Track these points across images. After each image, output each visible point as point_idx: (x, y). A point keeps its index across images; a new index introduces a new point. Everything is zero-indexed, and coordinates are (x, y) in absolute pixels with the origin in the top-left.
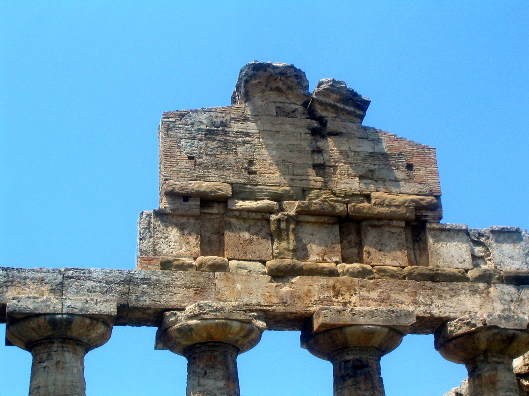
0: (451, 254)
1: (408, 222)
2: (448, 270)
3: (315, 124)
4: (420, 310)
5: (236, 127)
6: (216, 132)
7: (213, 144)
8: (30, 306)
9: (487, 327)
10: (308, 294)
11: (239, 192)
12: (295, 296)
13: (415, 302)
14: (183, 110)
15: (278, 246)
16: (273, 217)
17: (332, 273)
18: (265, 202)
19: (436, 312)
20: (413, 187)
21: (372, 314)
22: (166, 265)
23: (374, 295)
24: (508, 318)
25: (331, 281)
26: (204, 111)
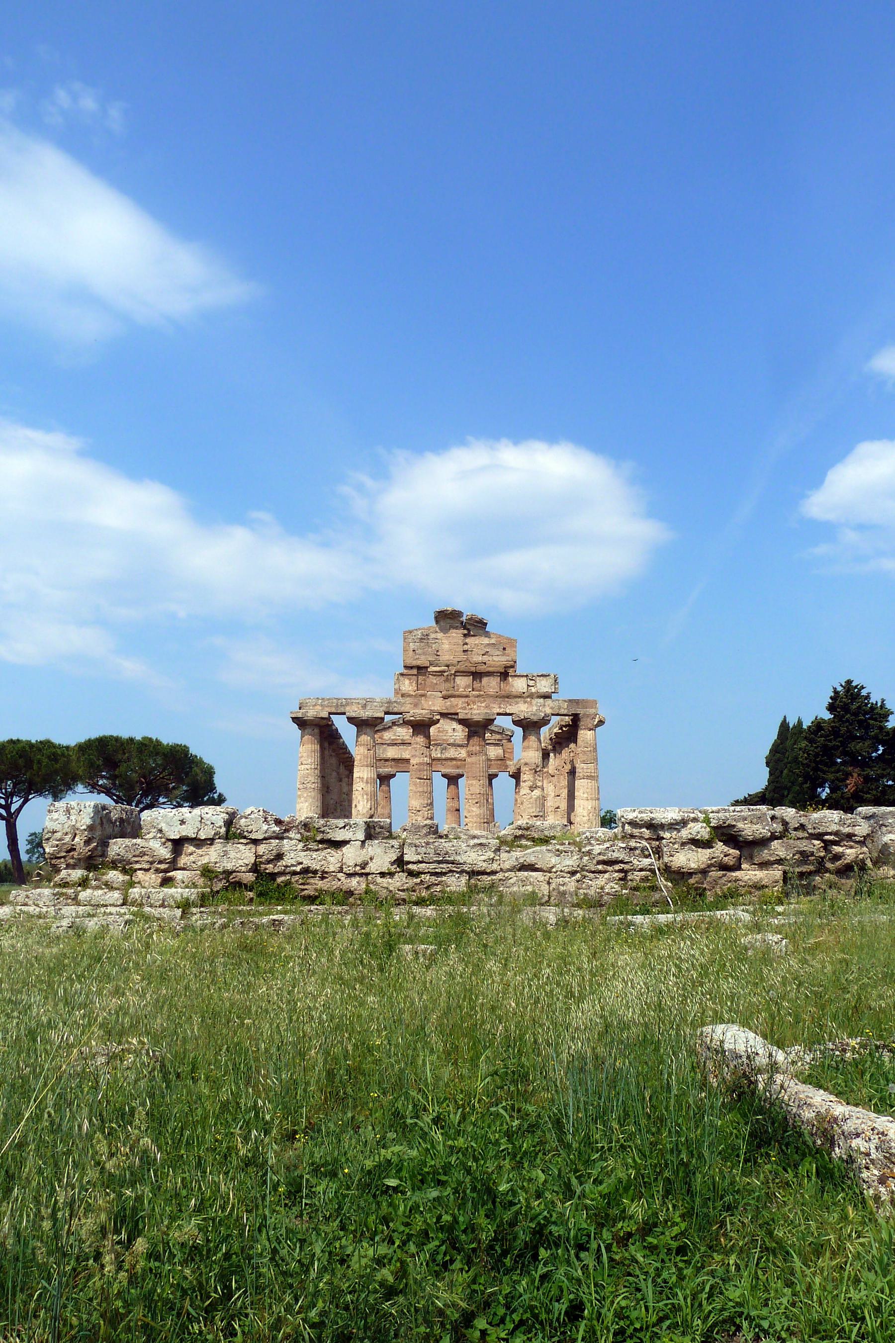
0: (519, 685)
1: (501, 673)
2: (514, 693)
3: (466, 632)
4: (501, 711)
5: (432, 636)
6: (424, 638)
7: (422, 644)
8: (353, 715)
9: (525, 719)
10: (457, 705)
11: (431, 664)
12: (452, 706)
13: (500, 707)
14: (411, 629)
15: (448, 685)
16: (445, 674)
17: (467, 696)
18: (443, 668)
19: (508, 712)
20: (504, 658)
21: (479, 714)
22: (403, 695)
23: (483, 705)
24: (534, 715)
25: (466, 700)
26: (420, 629)
